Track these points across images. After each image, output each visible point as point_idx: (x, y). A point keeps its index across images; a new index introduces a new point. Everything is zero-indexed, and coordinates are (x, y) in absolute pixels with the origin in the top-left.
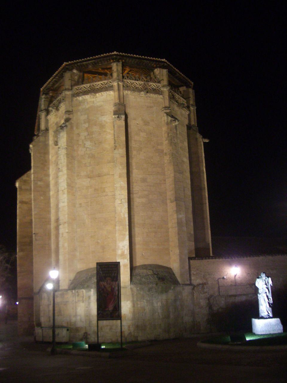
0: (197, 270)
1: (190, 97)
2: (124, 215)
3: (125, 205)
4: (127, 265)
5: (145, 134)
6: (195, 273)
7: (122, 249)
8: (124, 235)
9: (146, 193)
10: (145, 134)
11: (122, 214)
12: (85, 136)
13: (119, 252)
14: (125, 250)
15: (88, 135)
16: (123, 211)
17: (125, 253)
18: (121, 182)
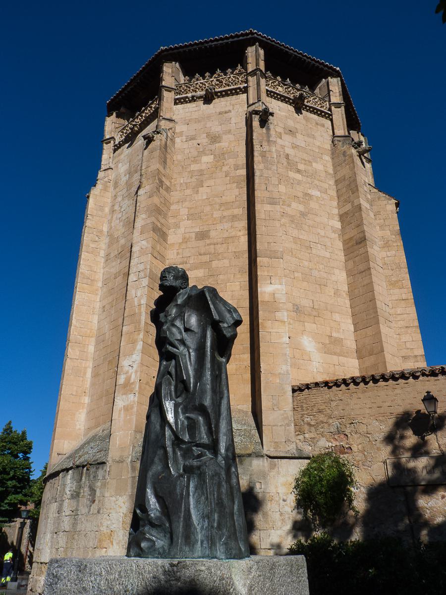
0: (320, 411)
1: (331, 91)
2: (140, 300)
3: (143, 283)
4: (132, 408)
5: (212, 157)
6: (312, 423)
7: (127, 372)
8: (134, 342)
9: (206, 258)
10: (212, 157)
11: (136, 300)
12: (123, 195)
13: (121, 380)
14: (132, 373)
15: (127, 190)
16: (139, 294)
17: (132, 381)
18: (144, 242)
